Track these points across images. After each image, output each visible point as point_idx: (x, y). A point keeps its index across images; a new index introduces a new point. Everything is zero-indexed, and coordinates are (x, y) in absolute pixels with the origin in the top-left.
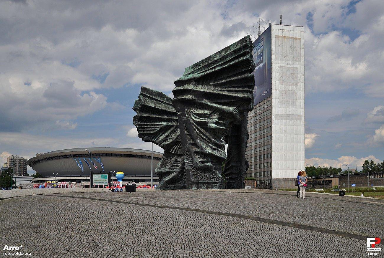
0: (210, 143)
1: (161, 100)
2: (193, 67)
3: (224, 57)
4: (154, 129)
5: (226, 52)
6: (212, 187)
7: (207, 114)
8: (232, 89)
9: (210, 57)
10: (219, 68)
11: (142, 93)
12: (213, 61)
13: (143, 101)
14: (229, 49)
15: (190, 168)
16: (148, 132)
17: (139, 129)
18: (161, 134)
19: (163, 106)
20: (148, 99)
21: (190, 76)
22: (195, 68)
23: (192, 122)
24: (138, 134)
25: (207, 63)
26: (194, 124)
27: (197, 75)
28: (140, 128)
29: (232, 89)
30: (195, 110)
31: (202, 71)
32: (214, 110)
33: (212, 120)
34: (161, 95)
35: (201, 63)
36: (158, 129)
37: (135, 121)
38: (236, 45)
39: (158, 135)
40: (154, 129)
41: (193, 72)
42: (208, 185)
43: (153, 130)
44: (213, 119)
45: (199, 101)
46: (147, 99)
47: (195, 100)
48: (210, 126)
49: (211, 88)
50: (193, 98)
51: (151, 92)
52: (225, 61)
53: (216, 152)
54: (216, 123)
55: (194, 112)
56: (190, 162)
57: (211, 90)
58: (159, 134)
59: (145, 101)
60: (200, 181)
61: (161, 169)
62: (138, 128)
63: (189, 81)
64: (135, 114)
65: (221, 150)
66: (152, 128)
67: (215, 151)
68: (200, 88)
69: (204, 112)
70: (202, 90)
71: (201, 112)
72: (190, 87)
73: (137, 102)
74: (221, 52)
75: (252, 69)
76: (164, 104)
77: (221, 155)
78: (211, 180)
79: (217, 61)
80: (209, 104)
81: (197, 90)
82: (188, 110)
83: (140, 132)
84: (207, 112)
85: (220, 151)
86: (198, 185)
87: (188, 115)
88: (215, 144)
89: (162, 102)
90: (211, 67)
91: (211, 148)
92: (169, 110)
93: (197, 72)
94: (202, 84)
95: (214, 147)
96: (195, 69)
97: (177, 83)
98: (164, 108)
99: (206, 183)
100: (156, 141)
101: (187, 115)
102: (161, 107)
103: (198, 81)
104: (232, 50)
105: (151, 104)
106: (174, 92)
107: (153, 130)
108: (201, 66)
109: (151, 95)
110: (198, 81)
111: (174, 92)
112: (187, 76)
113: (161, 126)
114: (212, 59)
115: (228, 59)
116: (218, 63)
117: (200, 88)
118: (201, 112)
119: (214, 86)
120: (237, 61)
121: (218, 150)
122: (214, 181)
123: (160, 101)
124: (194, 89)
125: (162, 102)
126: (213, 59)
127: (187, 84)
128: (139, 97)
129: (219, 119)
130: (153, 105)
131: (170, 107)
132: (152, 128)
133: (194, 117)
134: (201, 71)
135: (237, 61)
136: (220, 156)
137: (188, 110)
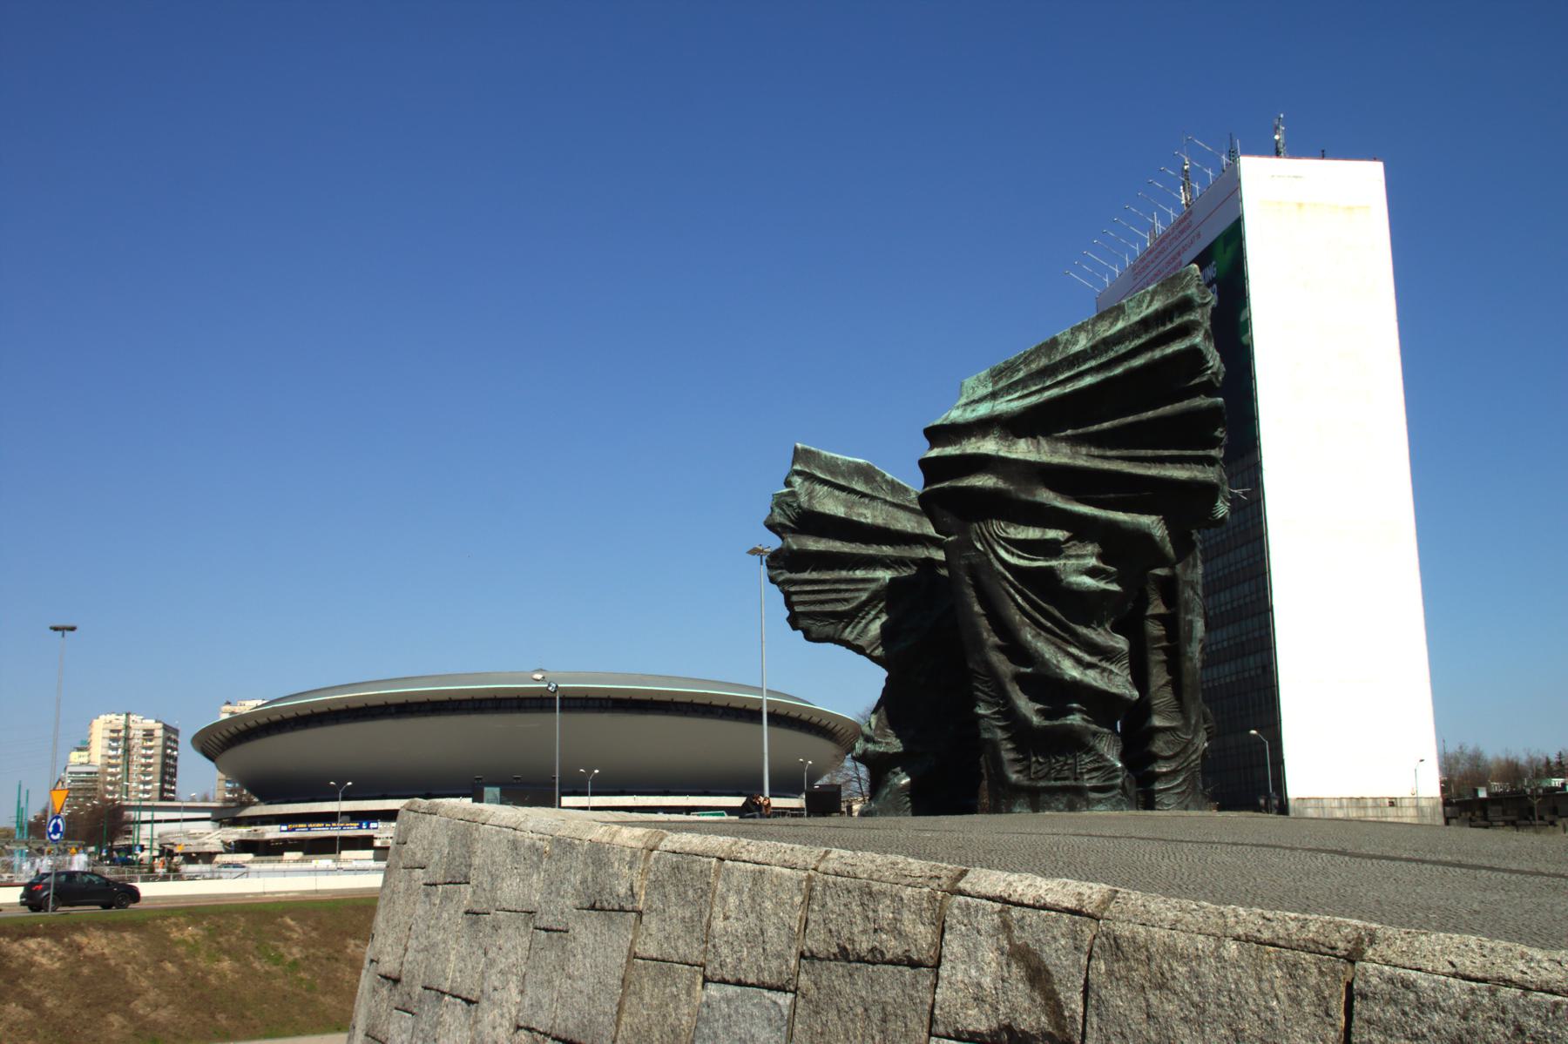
0: (1070, 643)
1: (868, 491)
2: (993, 377)
3: (1108, 343)
4: (847, 595)
5: (1112, 324)
6: (1090, 804)
7: (1055, 542)
8: (1142, 453)
9: (1053, 344)
10: (1088, 380)
11: (798, 467)
12: (1064, 355)
14: (1124, 313)
15: (1000, 734)
16: (828, 608)
17: (795, 598)
18: (873, 613)
19: (877, 513)
20: (821, 490)
21: (983, 410)
22: (1001, 379)
23: (1001, 568)
24: (787, 613)
25: (1044, 362)
26: (1006, 578)
27: (1008, 405)
28: (796, 593)
29: (1142, 453)
30: (1008, 526)
31: (1026, 392)
32: (1082, 529)
33: (1073, 561)
34: (867, 473)
35: (1021, 363)
36: (864, 596)
37: (776, 568)
38: (1148, 298)
39: (863, 618)
40: (847, 595)
41: (994, 396)
42: (1075, 797)
43: (846, 600)
44: (1078, 557)
45: (1023, 496)
46: (818, 487)
47: (1008, 492)
48: (1070, 584)
49: (1065, 448)
50: (1001, 484)
51: (831, 467)
52: (1112, 354)
53: (1098, 677)
54: (1092, 572)
55: (1004, 535)
56: (994, 713)
57: (1065, 455)
58: (868, 613)
60: (1042, 784)
61: (881, 742)
62: (788, 596)
63: (982, 427)
64: (773, 542)
65: (1112, 667)
66: (839, 591)
68: (1022, 450)
69: (1044, 533)
70: (1033, 457)
71: (1033, 533)
72: (989, 446)
73: (780, 502)
74: (1094, 325)
75: (1214, 380)
76: (879, 505)
77: (1117, 686)
78: (1086, 777)
80: (1060, 503)
81: (1014, 456)
82: (981, 528)
83: (798, 609)
85: (1111, 672)
86: (1036, 799)
87: (983, 546)
89: (873, 498)
90: (1061, 377)
91: (1078, 661)
92: (899, 527)
93: (1010, 394)
95: (1087, 658)
96: (1002, 384)
97: (936, 435)
98: (880, 521)
99: (1065, 790)
100: (856, 639)
101: (979, 546)
102: (869, 515)
103: (1012, 426)
104: (1135, 318)
105: (832, 505)
106: (925, 464)
107: (846, 600)
108: (1021, 374)
109: (832, 473)
110: (1012, 426)
111: (925, 464)
112: (969, 409)
113: (873, 586)
114: (1061, 348)
115: (1122, 349)
116: (1085, 361)
117: (1022, 450)
118: (1033, 533)
119: (1075, 441)
120: (1157, 354)
121: (1104, 670)
122: (1094, 783)
123: (863, 495)
124: (1002, 453)
125: (873, 498)
126: (1065, 347)
127: (975, 436)
128: (788, 484)
129: (1100, 557)
130: (840, 512)
131: (901, 514)
132: (839, 591)
133: (1007, 551)
134: (1023, 389)
135: (1157, 354)
136: (1114, 690)
137: (981, 528)
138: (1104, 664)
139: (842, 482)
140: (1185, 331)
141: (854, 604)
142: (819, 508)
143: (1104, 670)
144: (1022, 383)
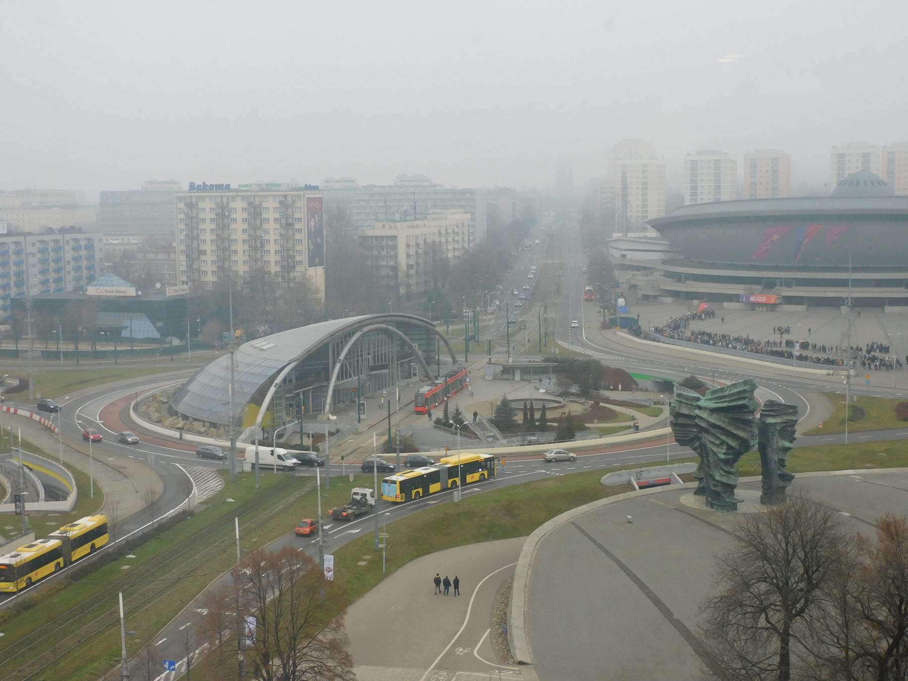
10: (725, 405)
13: (677, 409)
32: (723, 442)
36: (693, 436)
39: (693, 441)
54: (724, 454)
59: (679, 409)
67: (724, 477)
71: (713, 440)
79: (725, 397)
84: (717, 442)
85: (730, 477)
88: (725, 471)
94: (716, 413)
95: (723, 474)
109: (687, 400)
117: (713, 419)
124: (708, 419)
129: (727, 449)
138: (729, 475)
139: (690, 403)
140: (744, 398)
141: (690, 438)
142: (681, 411)
143: (728, 476)
144: (714, 399)
